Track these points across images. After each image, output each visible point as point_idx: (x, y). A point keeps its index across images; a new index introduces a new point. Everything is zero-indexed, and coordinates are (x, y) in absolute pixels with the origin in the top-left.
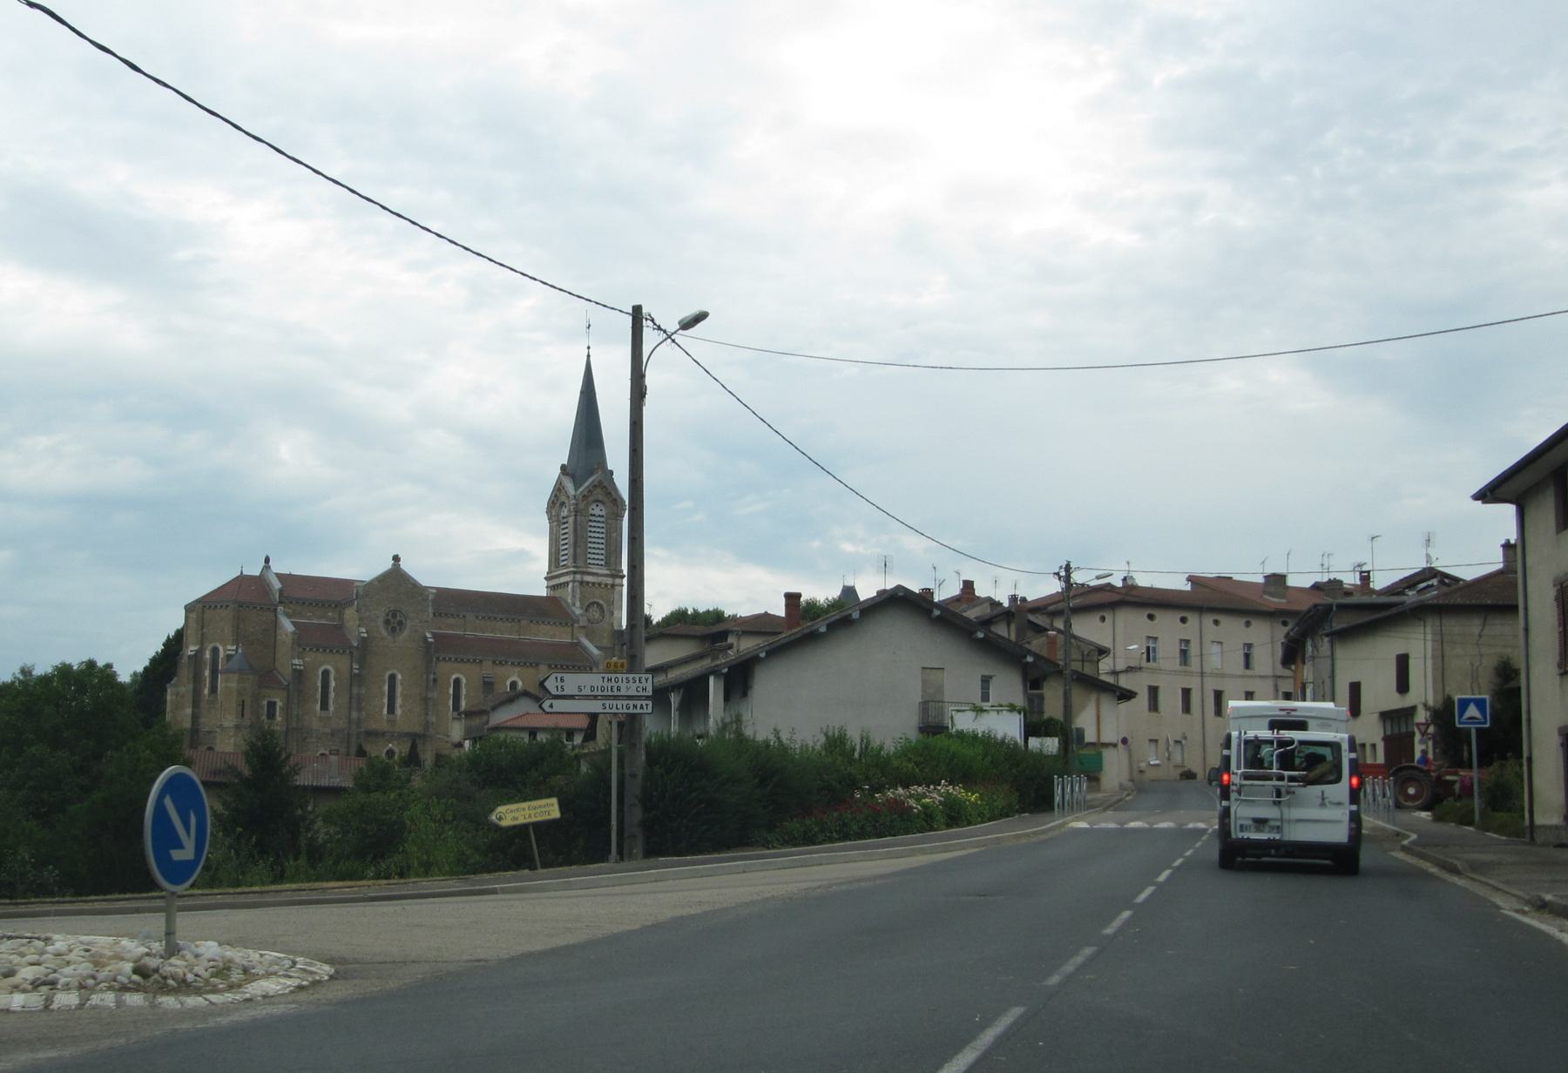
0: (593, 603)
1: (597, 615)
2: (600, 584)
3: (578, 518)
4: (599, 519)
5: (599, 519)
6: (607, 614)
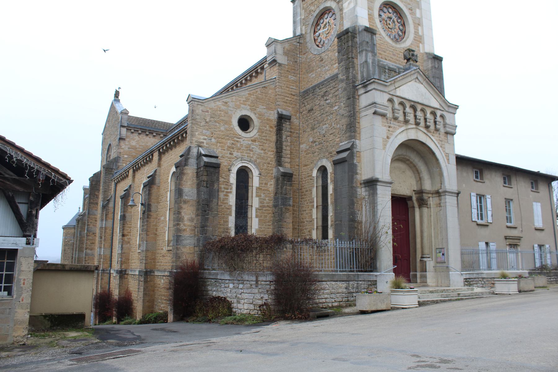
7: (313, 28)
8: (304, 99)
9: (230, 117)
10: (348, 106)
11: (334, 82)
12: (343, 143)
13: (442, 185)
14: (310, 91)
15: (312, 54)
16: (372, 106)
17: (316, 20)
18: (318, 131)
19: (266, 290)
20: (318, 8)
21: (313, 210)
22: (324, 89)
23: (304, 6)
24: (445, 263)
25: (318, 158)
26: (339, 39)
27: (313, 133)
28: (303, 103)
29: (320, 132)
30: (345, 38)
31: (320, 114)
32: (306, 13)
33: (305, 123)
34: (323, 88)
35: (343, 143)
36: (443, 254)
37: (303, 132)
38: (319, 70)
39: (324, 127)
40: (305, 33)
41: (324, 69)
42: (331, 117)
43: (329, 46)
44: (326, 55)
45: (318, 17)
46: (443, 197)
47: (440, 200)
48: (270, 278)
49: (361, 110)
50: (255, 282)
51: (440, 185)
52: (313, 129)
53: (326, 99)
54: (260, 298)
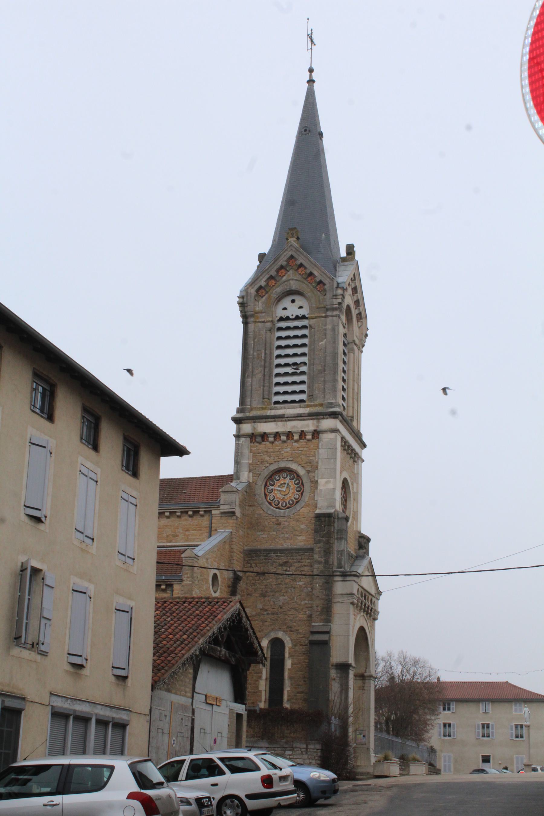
0: (280, 471)
1: (292, 493)
2: (289, 435)
3: (251, 326)
4: (299, 323)
5: (299, 323)
6: (307, 486)
7: (265, 480)
8: (250, 558)
9: (208, 575)
10: (326, 590)
11: (300, 556)
12: (316, 624)
13: (367, 671)
14: (261, 553)
15: (264, 511)
16: (350, 596)
17: (271, 473)
18: (272, 600)
19: (313, 757)
20: (277, 463)
21: (260, 681)
22: (283, 558)
23: (253, 449)
24: (366, 744)
25: (270, 628)
26: (318, 518)
27: (263, 600)
28: (248, 563)
29: (274, 602)
30: (325, 521)
31: (276, 583)
32: (255, 458)
33: (251, 586)
34: (282, 556)
35: (316, 624)
36: (364, 736)
37: (248, 595)
38: (275, 533)
39: (281, 598)
40: (253, 482)
41: (283, 535)
42: (293, 591)
43: (293, 513)
44: (286, 521)
45: (273, 472)
46: (367, 681)
47: (364, 683)
48: (318, 746)
49: (335, 596)
50: (304, 750)
51: (365, 669)
52: (263, 595)
53: (287, 569)
54: (309, 763)
